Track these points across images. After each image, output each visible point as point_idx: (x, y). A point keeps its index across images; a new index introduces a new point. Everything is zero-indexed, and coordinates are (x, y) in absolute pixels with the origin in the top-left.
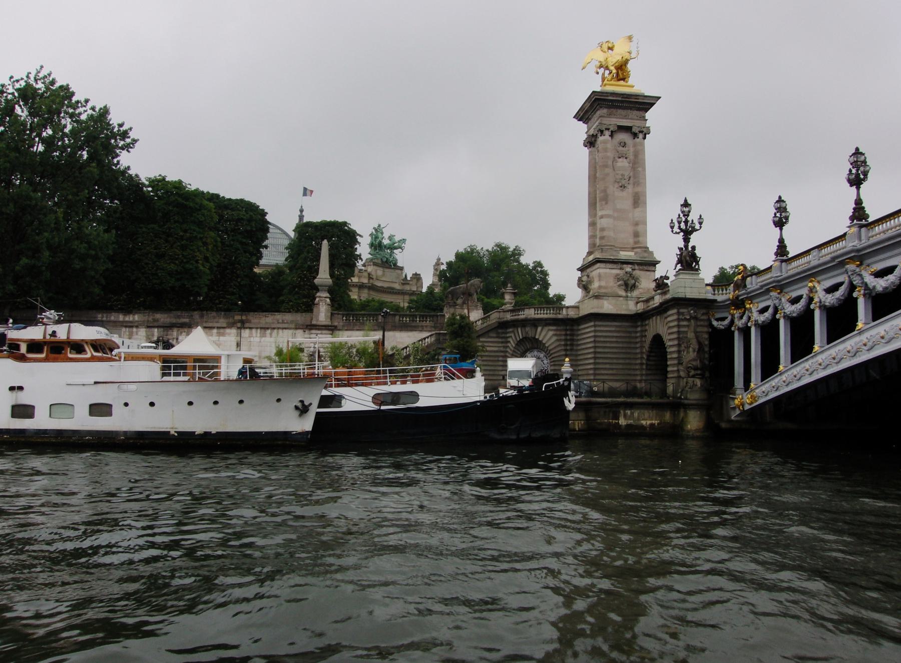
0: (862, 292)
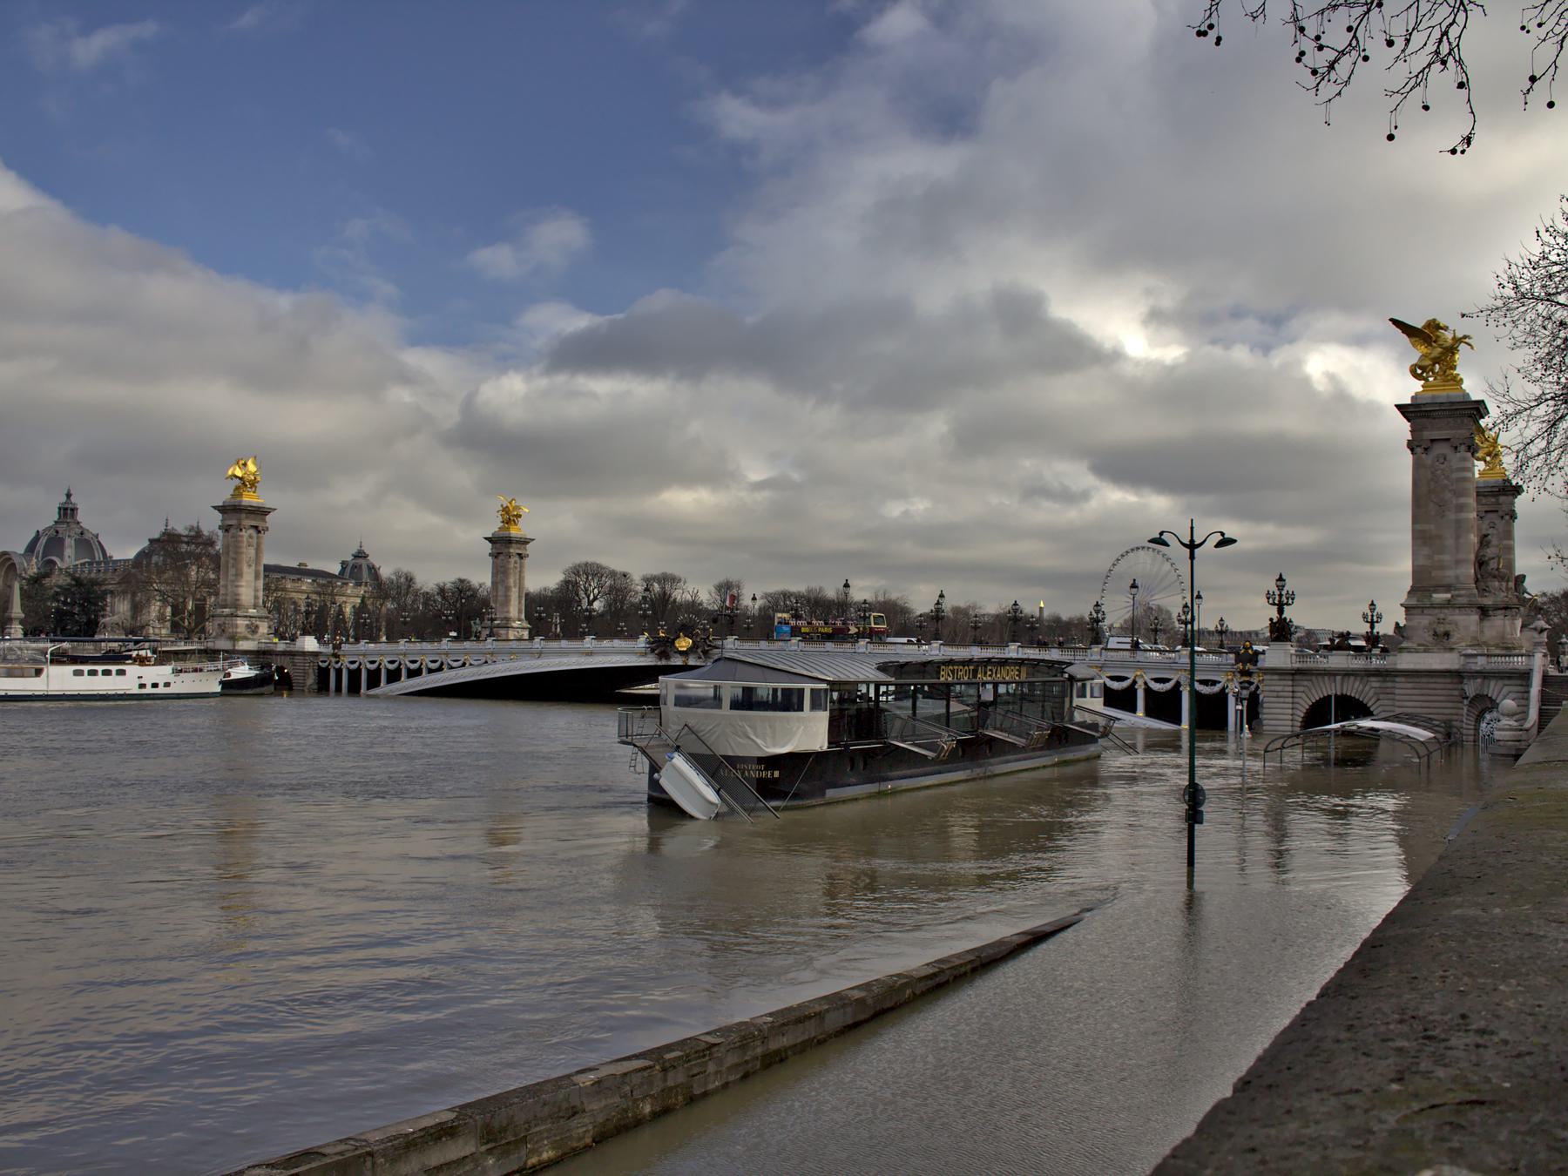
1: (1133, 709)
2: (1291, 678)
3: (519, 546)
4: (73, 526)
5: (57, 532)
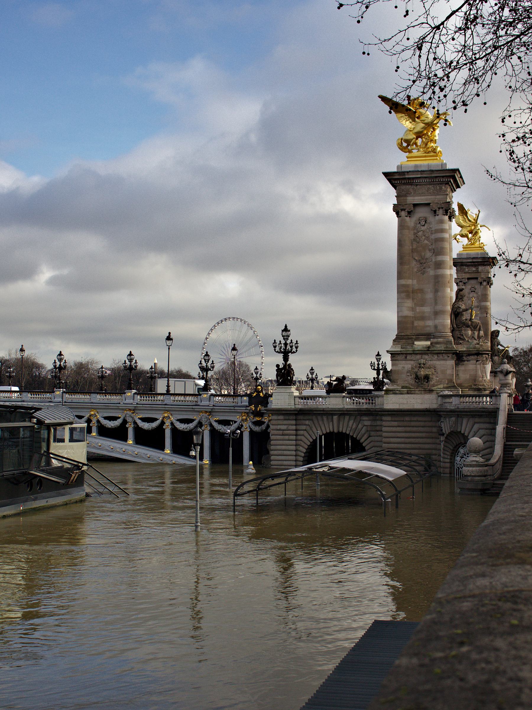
1: (162, 448)
2: (294, 417)
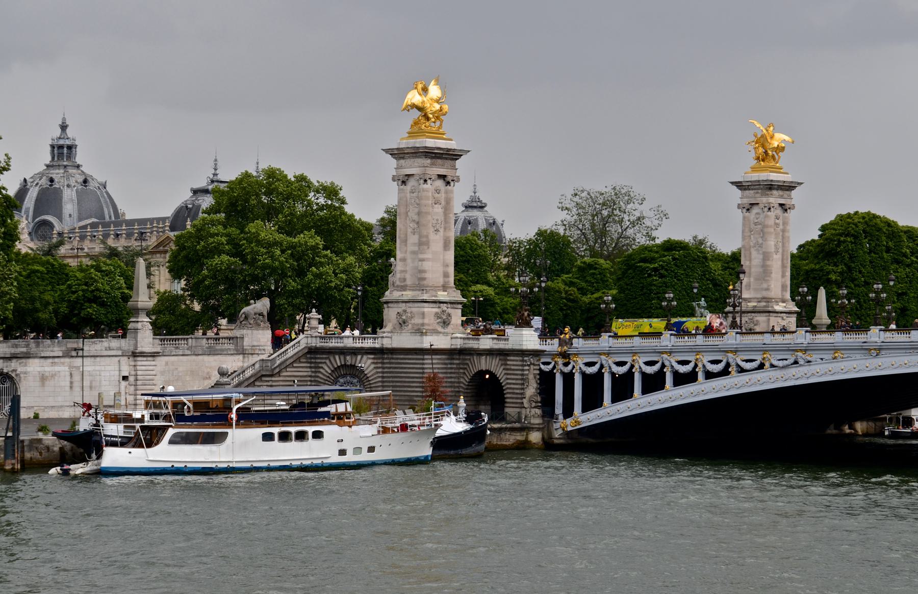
0: (670, 370)
3: (781, 193)
4: (72, 171)
5: (52, 180)
